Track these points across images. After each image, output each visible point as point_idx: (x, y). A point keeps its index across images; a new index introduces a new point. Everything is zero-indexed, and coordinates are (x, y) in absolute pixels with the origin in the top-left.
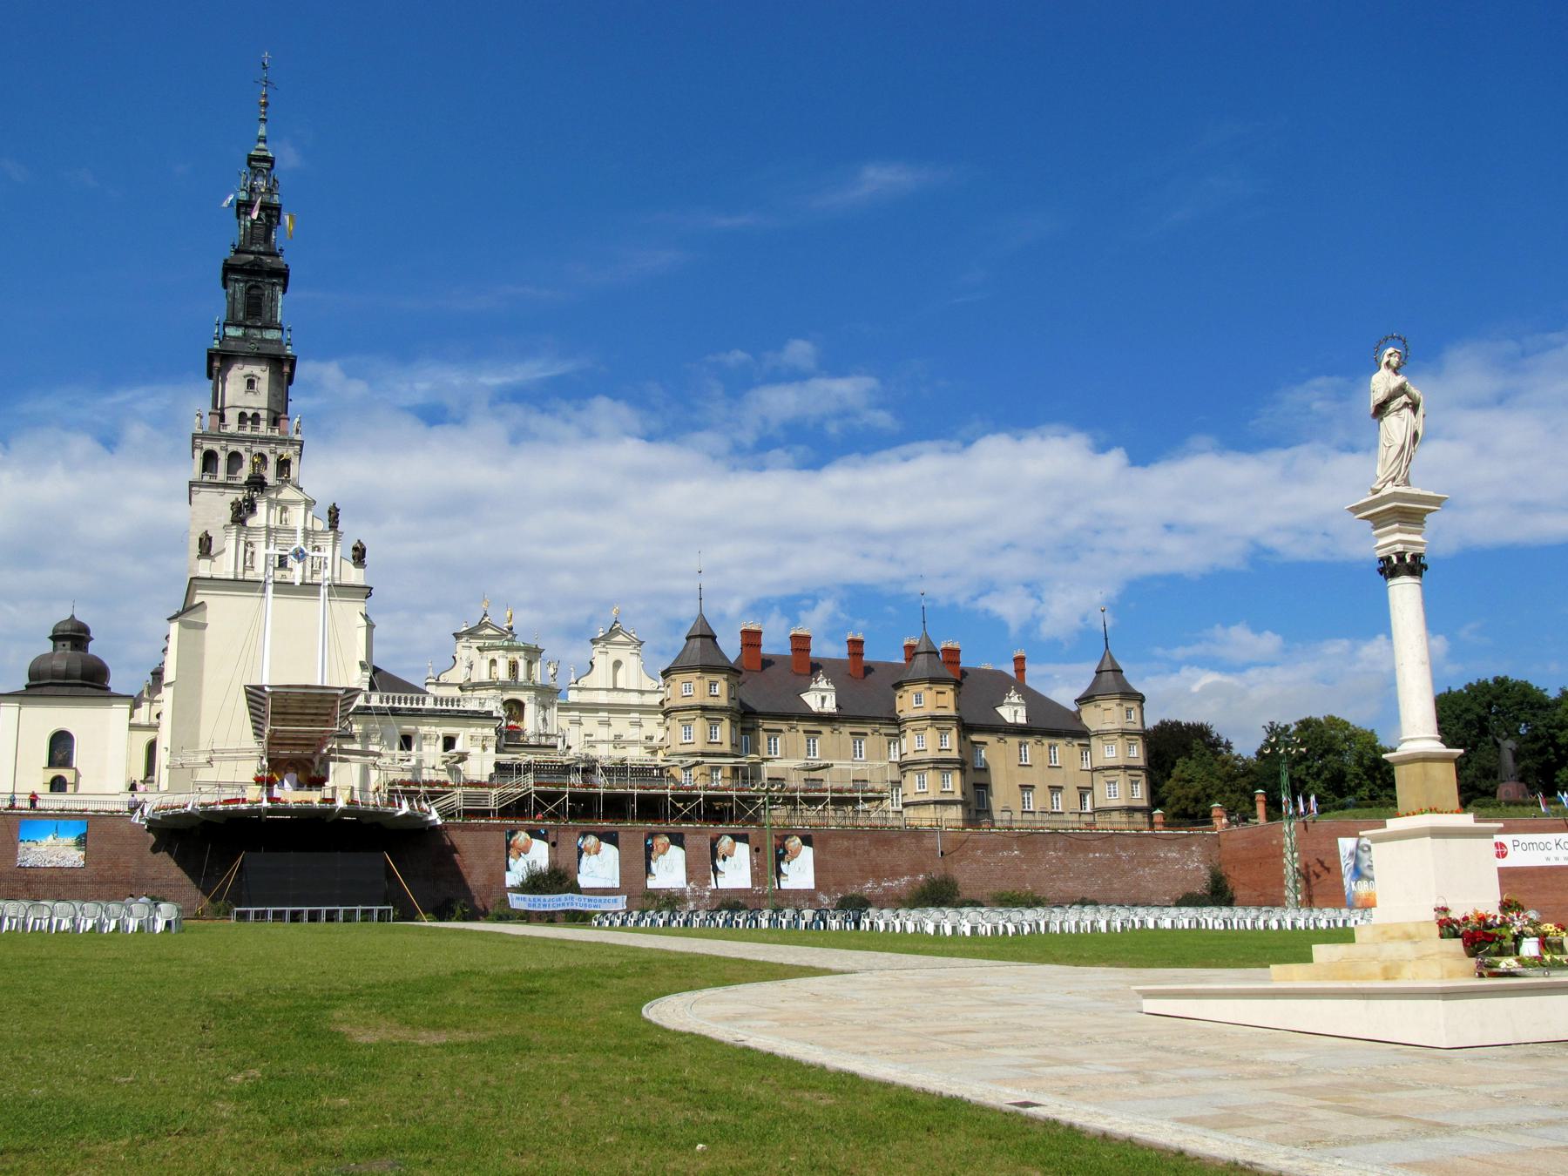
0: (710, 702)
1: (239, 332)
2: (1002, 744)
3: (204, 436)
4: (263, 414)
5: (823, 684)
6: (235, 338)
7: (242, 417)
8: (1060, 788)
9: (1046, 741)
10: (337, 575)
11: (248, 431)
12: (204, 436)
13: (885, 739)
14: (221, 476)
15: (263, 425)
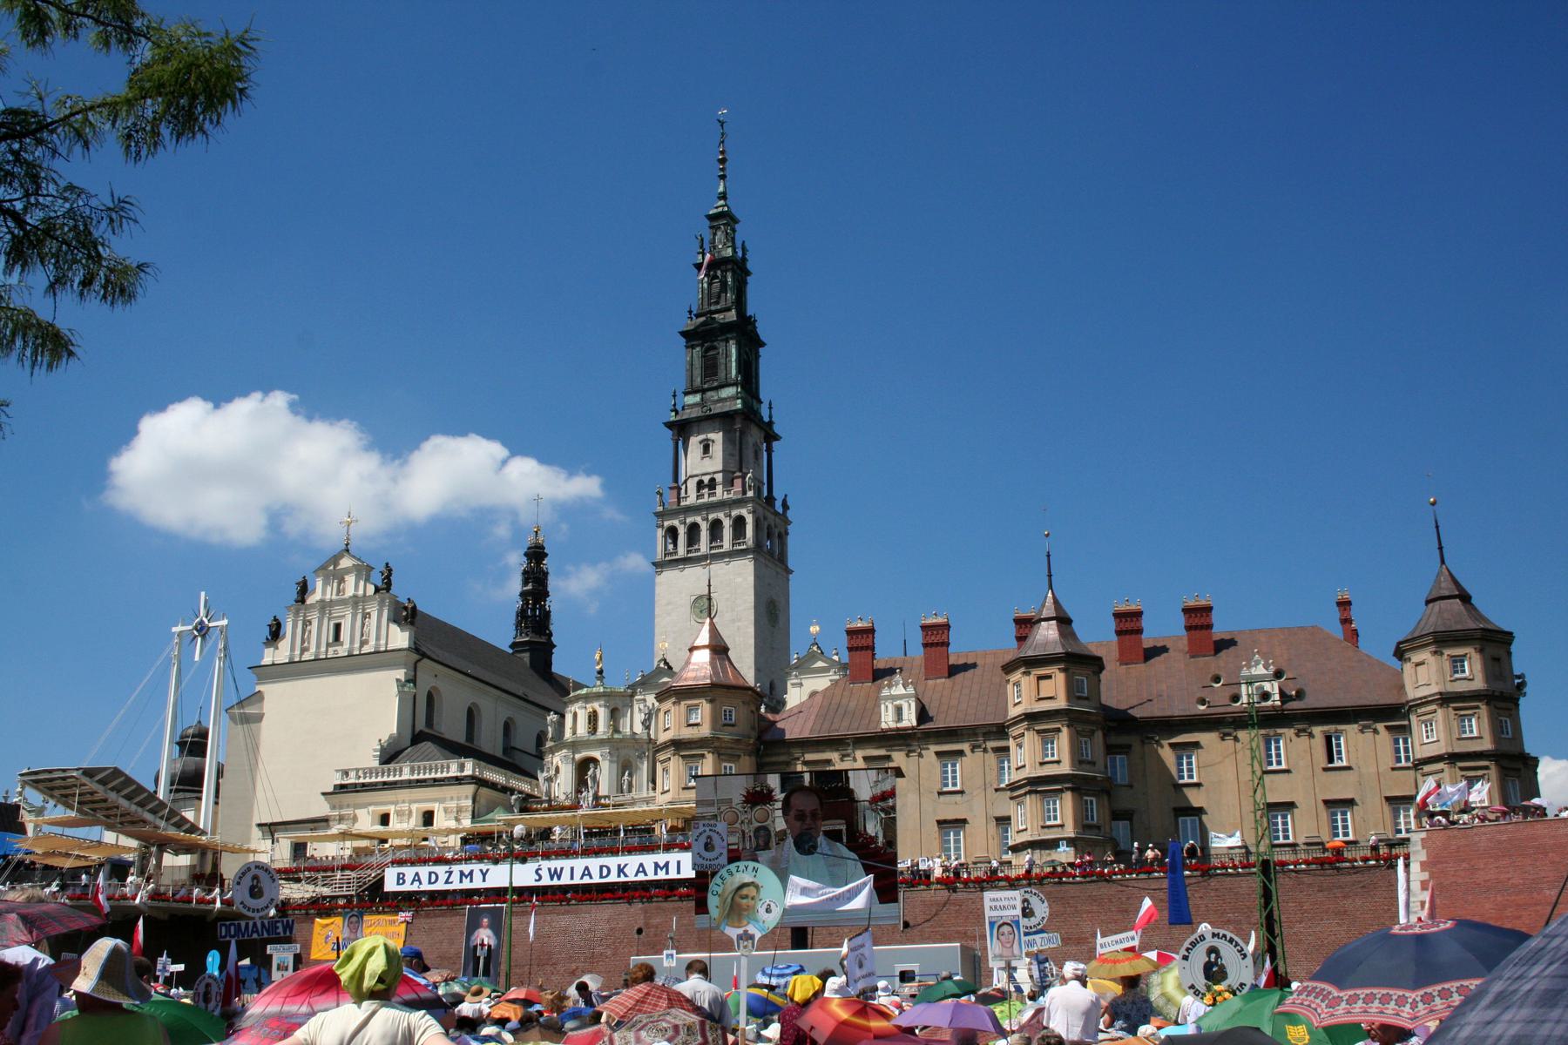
0: (688, 733)
1: (696, 398)
2: (1229, 742)
3: (661, 515)
4: (719, 478)
5: (899, 690)
6: (692, 406)
7: (700, 485)
8: (1349, 803)
9: (1317, 730)
10: (383, 642)
11: (706, 499)
12: (661, 515)
13: (991, 758)
14: (682, 551)
15: (719, 489)
